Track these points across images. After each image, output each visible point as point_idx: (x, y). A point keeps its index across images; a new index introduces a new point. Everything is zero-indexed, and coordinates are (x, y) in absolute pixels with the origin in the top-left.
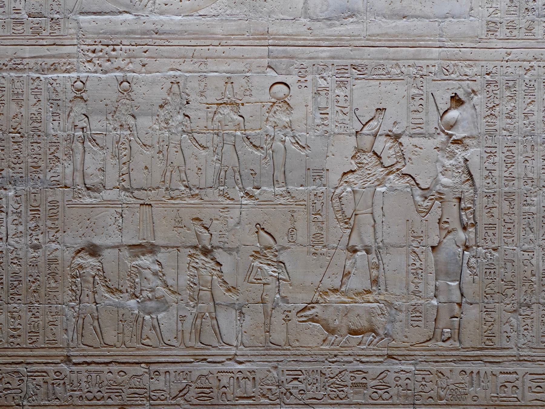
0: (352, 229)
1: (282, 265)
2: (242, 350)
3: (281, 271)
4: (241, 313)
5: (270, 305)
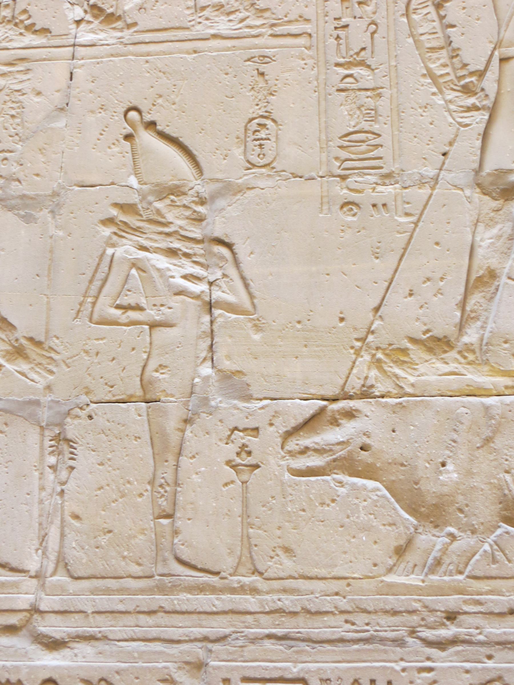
0: (493, 112)
1: (224, 251)
2: (62, 590)
3: (219, 274)
4: (61, 439)
5: (174, 411)
